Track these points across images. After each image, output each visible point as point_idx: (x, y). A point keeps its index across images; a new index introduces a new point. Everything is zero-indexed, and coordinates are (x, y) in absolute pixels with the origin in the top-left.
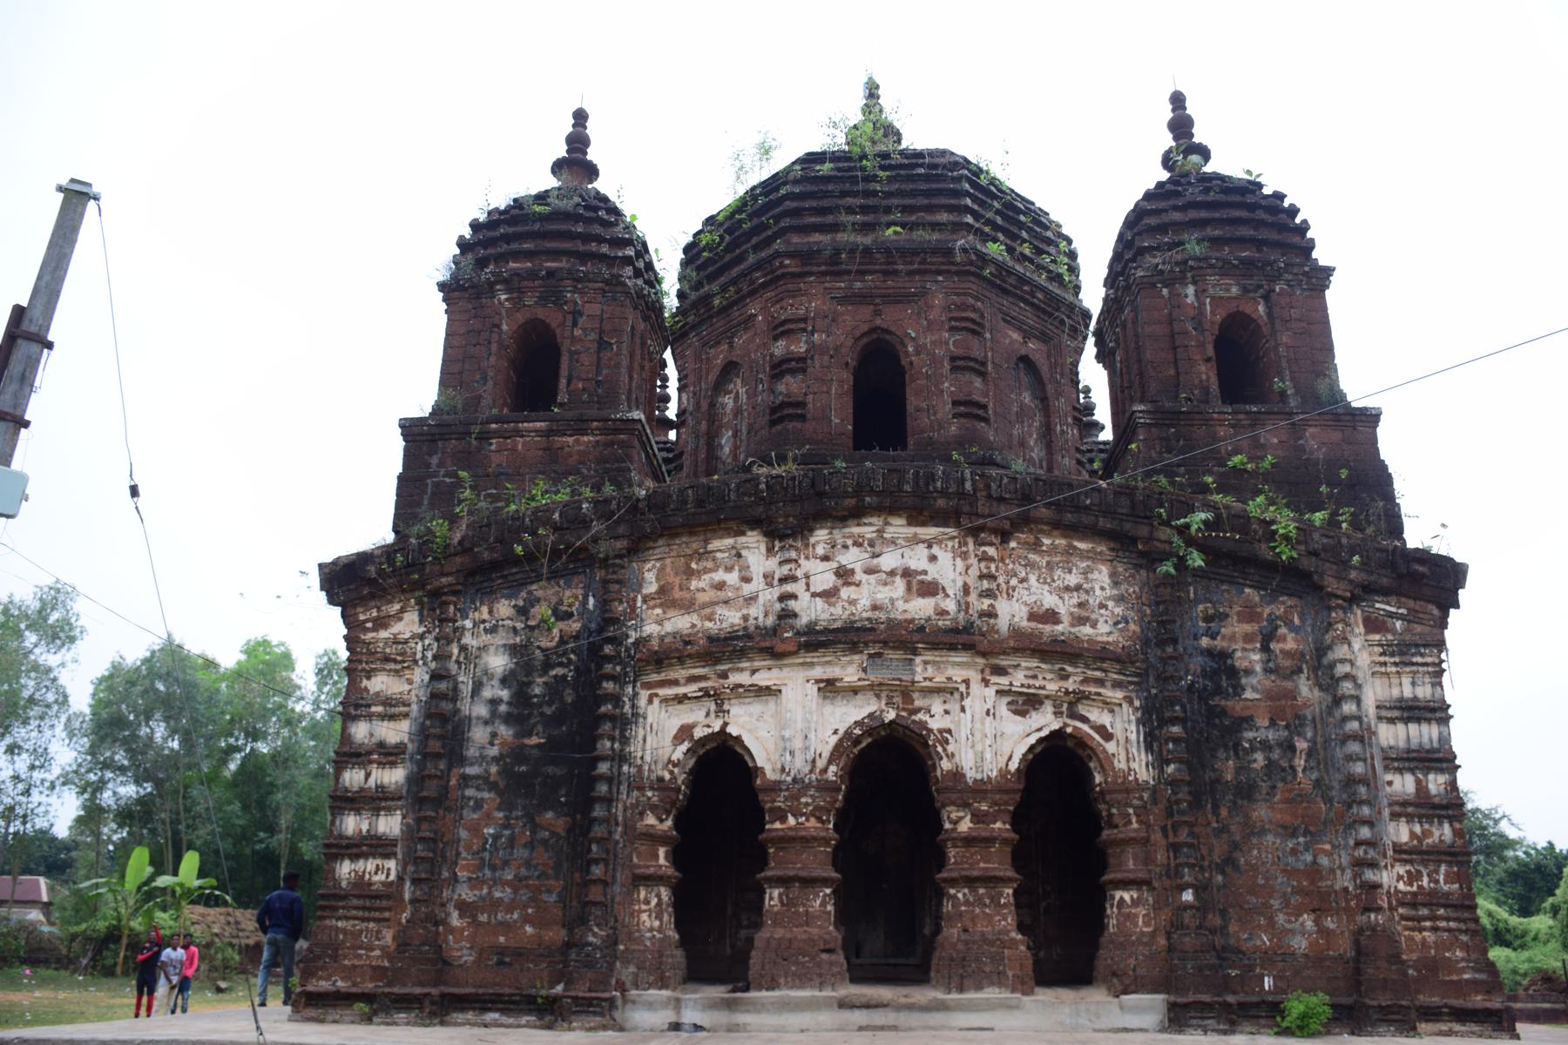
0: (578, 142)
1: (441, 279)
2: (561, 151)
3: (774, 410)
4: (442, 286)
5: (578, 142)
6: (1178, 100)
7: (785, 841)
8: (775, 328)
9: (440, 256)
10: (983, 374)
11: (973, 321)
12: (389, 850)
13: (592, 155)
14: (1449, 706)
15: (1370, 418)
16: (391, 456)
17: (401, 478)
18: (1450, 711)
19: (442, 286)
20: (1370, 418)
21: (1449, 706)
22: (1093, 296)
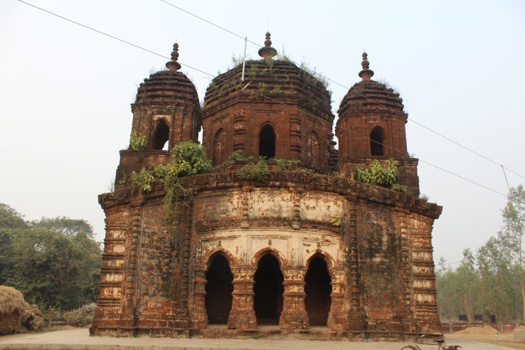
0: (175, 55)
1: (133, 103)
2: (169, 59)
3: (235, 146)
4: (131, 104)
5: (175, 55)
6: (365, 56)
7: (238, 283)
8: (236, 118)
9: (132, 97)
10: (300, 137)
11: (297, 119)
12: (120, 285)
13: (179, 61)
14: (433, 248)
15: (415, 161)
16: (116, 161)
17: (119, 167)
18: (433, 249)
19: (131, 104)
20: (415, 161)
21: (433, 248)
22: (335, 107)
